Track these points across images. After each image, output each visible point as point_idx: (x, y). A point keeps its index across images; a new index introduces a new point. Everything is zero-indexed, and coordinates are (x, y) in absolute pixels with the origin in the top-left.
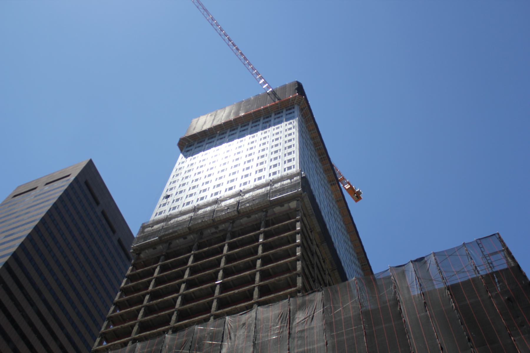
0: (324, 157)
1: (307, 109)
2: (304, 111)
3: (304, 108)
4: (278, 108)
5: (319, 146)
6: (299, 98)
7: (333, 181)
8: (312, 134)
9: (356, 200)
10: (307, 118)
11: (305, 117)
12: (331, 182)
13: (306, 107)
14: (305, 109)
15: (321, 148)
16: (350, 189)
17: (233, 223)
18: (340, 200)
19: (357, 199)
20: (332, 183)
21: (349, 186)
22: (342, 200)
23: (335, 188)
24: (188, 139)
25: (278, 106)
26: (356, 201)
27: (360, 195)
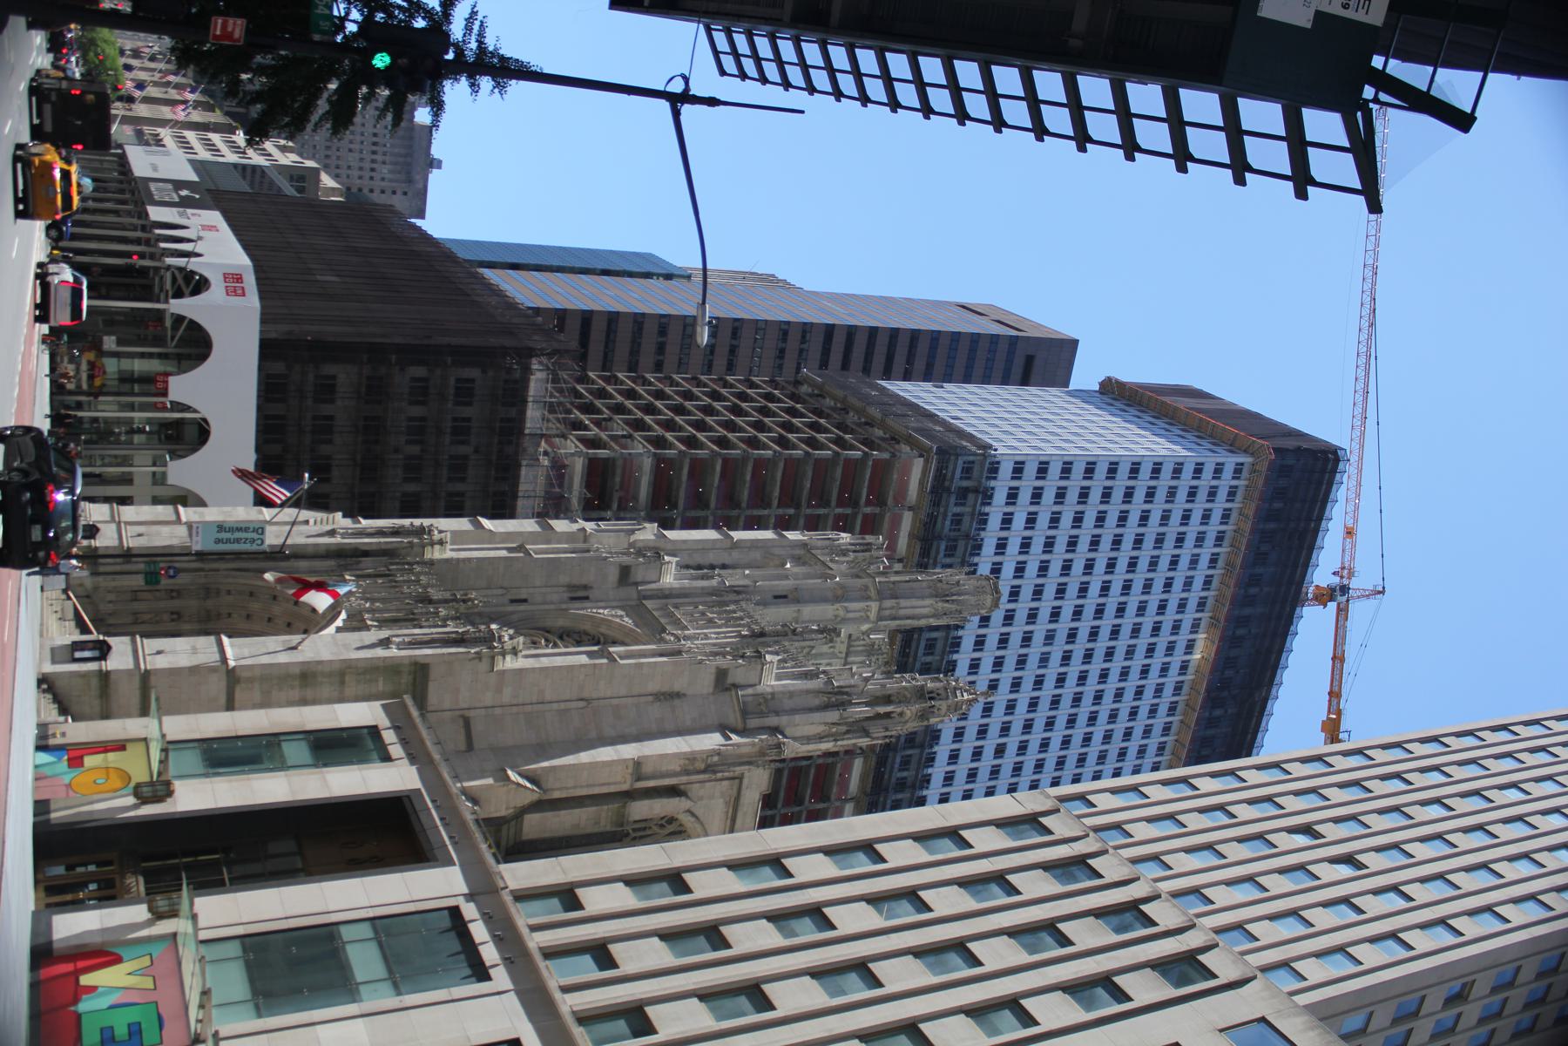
17: (866, 424)
21: (1334, 716)
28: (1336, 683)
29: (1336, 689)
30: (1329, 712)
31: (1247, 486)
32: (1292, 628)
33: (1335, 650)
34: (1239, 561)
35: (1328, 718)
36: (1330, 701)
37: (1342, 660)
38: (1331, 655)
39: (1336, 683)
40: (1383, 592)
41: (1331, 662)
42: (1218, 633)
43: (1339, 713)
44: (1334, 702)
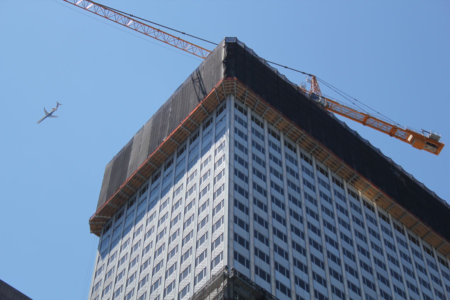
0: (316, 149)
1: (248, 93)
2: (246, 98)
3: (245, 95)
4: (205, 113)
5: (299, 137)
6: (228, 85)
7: (351, 176)
8: (278, 125)
9: (434, 151)
10: (256, 106)
11: (254, 106)
12: (349, 179)
13: (245, 92)
14: (247, 95)
15: (304, 138)
16: (415, 141)
18: (379, 198)
19: (435, 149)
20: (352, 179)
21: (411, 137)
22: (382, 196)
23: (361, 184)
24: (101, 216)
25: (204, 111)
26: (436, 153)
27: (437, 141)
28: (384, 128)
29: (389, 129)
30: (405, 140)
31: (252, 110)
32: (353, 133)
33: (358, 121)
34: (310, 140)
35: (411, 143)
36: (397, 137)
37: (368, 117)
38: (361, 125)
39: (384, 128)
40: (314, 78)
41: (366, 127)
42: (362, 179)
43: (409, 132)
44: (399, 133)
